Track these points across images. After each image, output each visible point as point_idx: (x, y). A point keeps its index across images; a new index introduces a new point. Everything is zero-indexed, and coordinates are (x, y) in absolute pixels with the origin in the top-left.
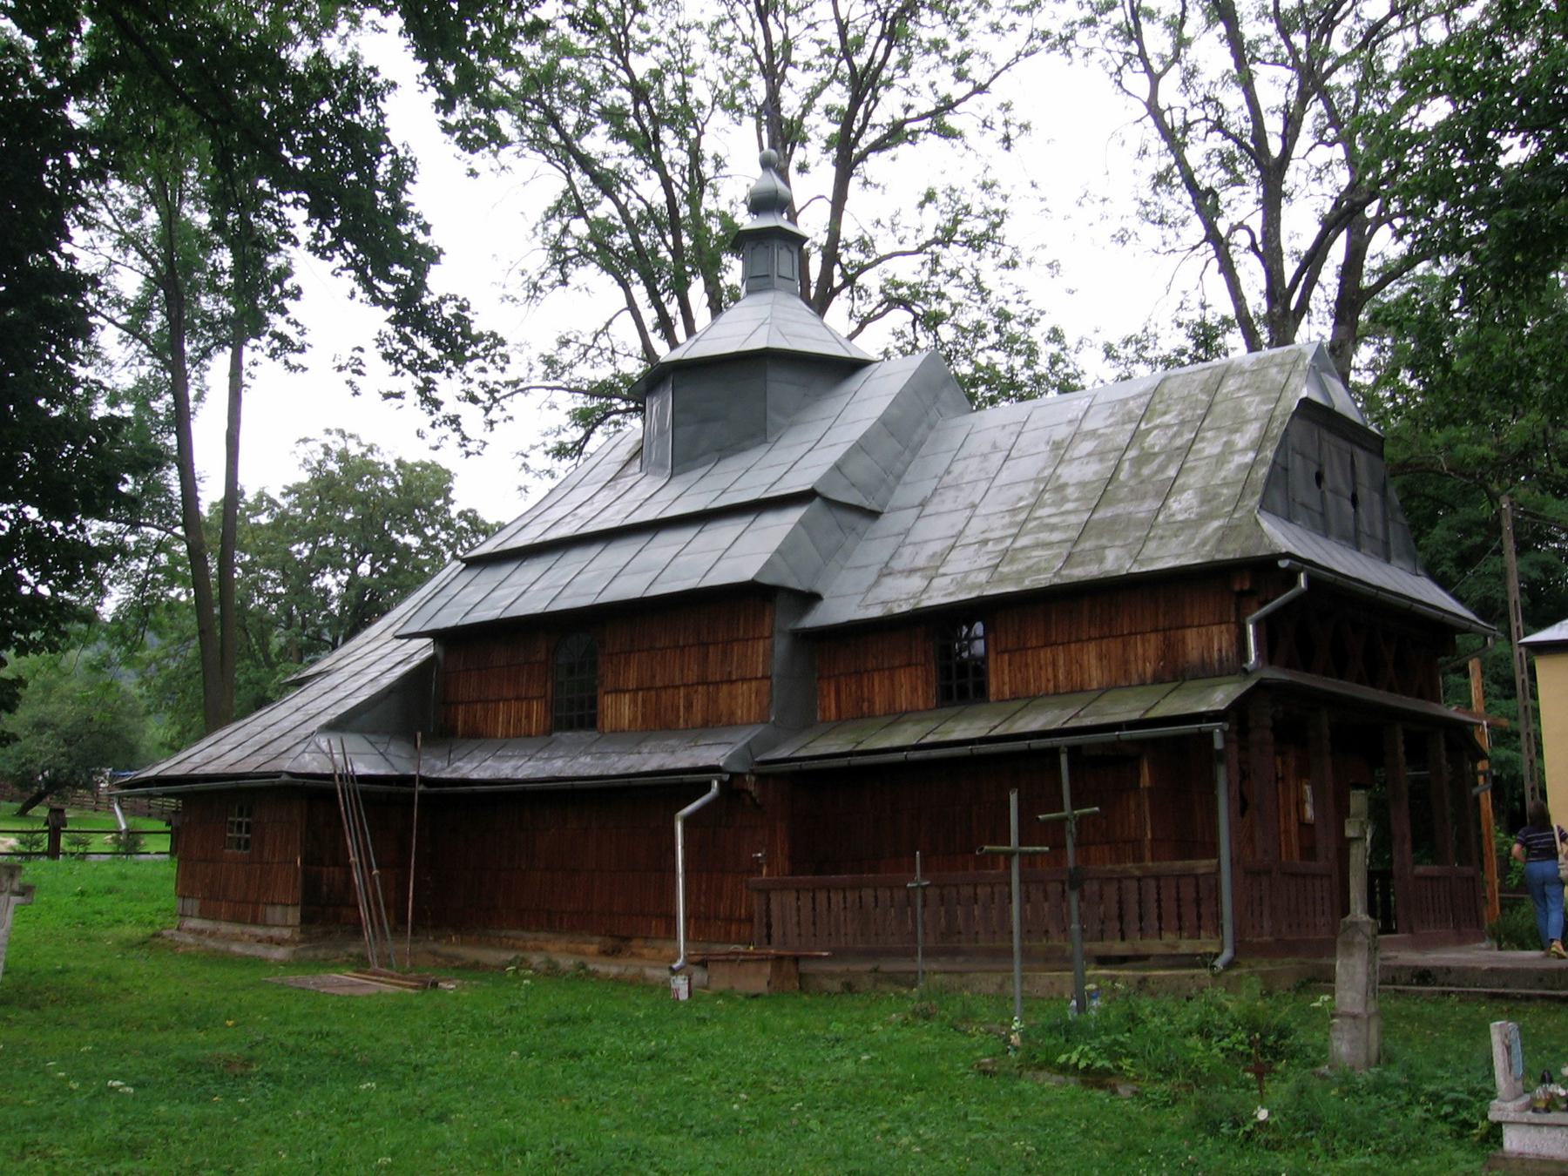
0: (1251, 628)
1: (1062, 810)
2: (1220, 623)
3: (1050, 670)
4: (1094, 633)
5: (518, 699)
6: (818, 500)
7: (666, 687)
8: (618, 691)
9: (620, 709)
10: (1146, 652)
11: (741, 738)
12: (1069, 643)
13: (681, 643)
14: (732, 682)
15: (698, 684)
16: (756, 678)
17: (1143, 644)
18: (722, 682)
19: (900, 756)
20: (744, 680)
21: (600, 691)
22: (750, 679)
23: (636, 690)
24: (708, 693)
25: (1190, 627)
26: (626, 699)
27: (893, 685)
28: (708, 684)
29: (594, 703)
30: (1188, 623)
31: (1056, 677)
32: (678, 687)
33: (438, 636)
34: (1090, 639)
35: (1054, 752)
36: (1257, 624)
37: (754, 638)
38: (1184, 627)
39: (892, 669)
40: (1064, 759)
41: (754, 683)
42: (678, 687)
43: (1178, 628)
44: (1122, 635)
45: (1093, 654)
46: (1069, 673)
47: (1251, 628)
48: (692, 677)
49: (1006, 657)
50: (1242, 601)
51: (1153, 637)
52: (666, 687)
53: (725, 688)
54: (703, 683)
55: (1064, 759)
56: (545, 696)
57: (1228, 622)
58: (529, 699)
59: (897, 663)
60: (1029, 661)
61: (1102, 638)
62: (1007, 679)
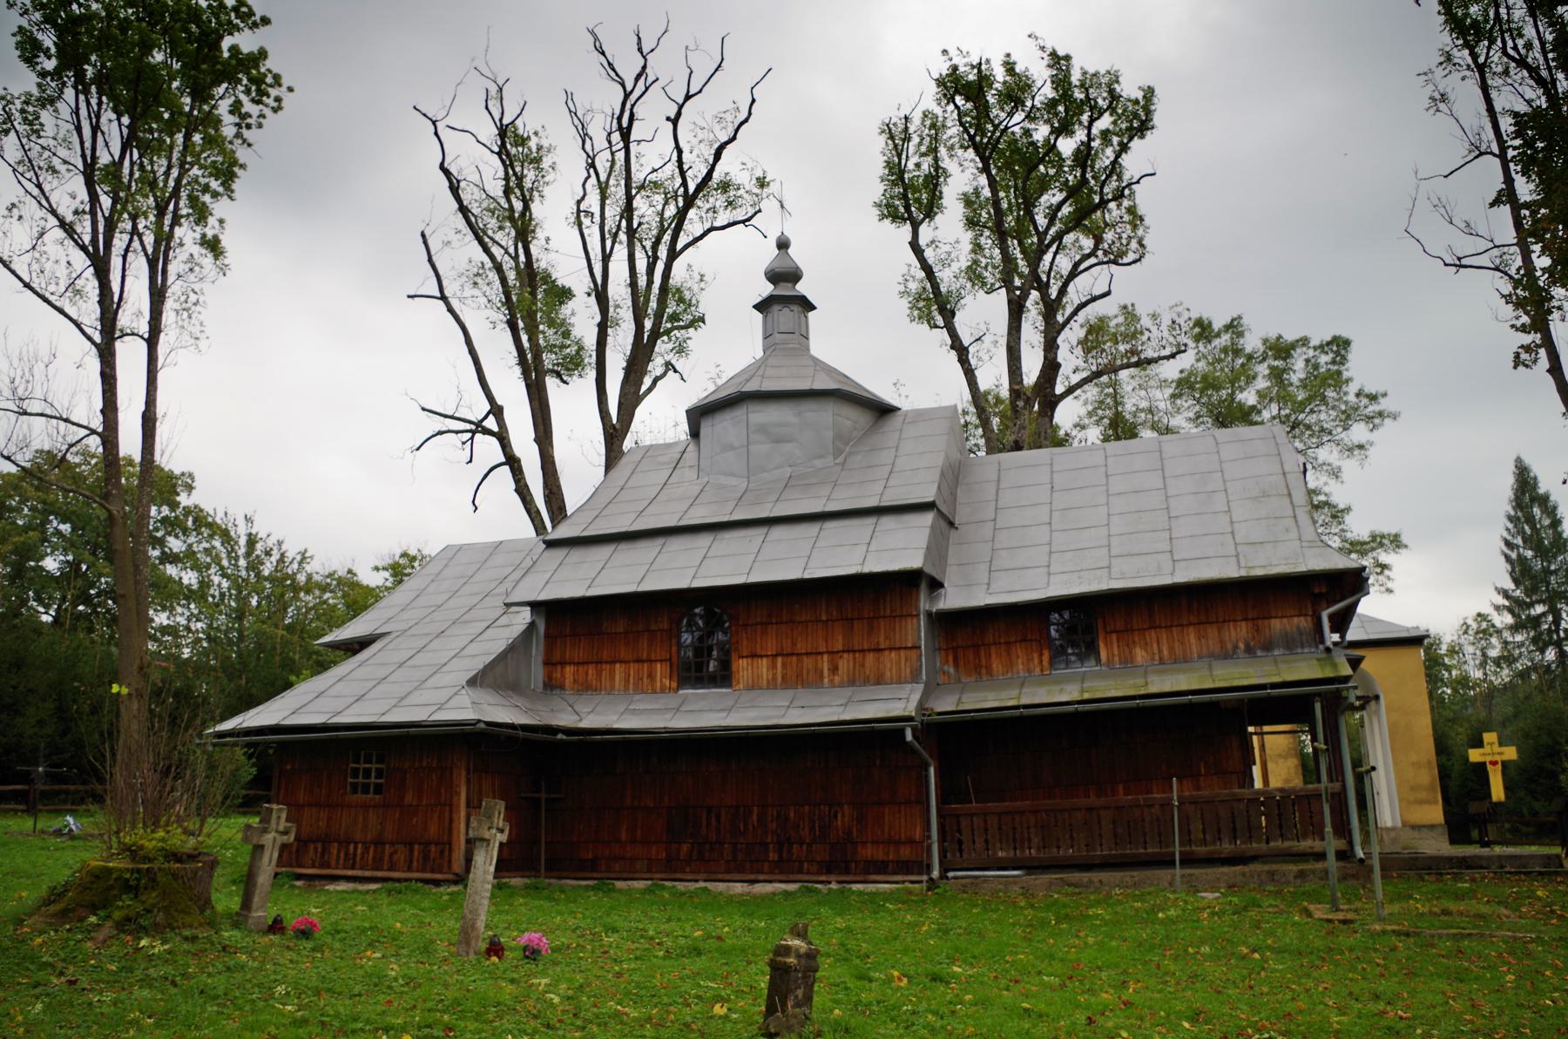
3: (1155, 645)
4: (1193, 619)
5: (638, 661)
7: (807, 654)
8: (753, 656)
10: (1239, 632)
13: (824, 618)
16: (906, 648)
18: (869, 650)
19: (1016, 712)
20: (891, 649)
21: (734, 656)
22: (900, 648)
24: (854, 659)
26: (764, 663)
28: (854, 651)
31: (1160, 651)
32: (821, 653)
33: (535, 606)
34: (1190, 624)
37: (901, 616)
38: (1270, 618)
39: (1008, 643)
40: (1318, 706)
41: (902, 652)
42: (821, 653)
43: (1264, 618)
51: (1243, 623)
52: (807, 654)
53: (870, 657)
54: (848, 651)
55: (1318, 706)
56: (670, 660)
57: (1306, 615)
59: (1013, 639)
62: (1116, 652)
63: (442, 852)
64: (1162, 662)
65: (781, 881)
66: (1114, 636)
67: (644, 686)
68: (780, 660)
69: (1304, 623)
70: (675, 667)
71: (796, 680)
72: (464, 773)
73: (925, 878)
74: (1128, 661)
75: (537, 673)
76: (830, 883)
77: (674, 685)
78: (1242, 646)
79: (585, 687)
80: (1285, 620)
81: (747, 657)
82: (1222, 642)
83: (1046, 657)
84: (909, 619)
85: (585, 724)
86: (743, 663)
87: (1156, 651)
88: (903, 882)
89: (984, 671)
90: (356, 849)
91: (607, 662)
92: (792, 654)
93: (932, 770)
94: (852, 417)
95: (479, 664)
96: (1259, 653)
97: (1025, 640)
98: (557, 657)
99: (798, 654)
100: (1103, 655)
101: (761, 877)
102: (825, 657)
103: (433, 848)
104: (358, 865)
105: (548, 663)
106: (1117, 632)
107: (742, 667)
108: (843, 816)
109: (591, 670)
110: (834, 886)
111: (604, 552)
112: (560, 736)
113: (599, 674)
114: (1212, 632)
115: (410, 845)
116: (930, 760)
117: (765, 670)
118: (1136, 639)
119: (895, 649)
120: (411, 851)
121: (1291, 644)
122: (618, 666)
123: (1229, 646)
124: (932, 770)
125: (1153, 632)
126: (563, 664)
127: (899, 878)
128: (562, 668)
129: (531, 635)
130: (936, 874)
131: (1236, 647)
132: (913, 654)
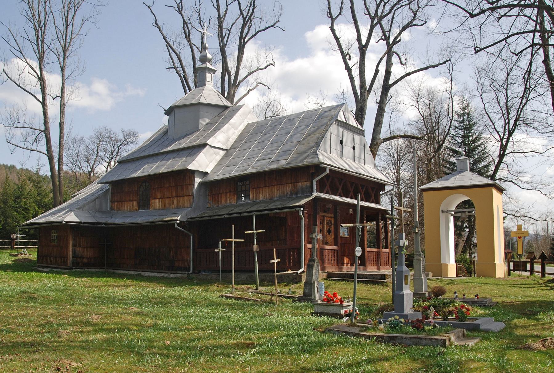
0: (315, 183)
1: (253, 230)
2: (307, 181)
5: (130, 201)
6: (208, 146)
7: (167, 198)
8: (155, 199)
9: (155, 203)
11: (185, 212)
12: (270, 186)
14: (184, 196)
15: (175, 197)
17: (288, 187)
20: (186, 196)
21: (151, 199)
23: (160, 199)
25: (300, 182)
26: (157, 201)
27: (226, 197)
28: (178, 197)
29: (149, 201)
30: (299, 181)
31: (266, 195)
36: (316, 182)
38: (298, 182)
42: (170, 197)
43: (297, 183)
44: (283, 184)
45: (276, 189)
46: (269, 194)
47: (315, 183)
48: (174, 195)
49: (254, 189)
50: (313, 176)
51: (291, 184)
54: (176, 197)
58: (133, 201)
60: (260, 191)
61: (278, 185)
62: (254, 196)
69: (308, 183)
72: (71, 237)
73: (187, 273)
78: (289, 193)
86: (153, 200)
87: (265, 195)
89: (219, 203)
91: (124, 201)
92: (164, 198)
93: (191, 237)
94: (219, 110)
97: (230, 192)
99: (165, 198)
101: (154, 271)
106: (255, 188)
112: (103, 225)
113: (122, 204)
114: (281, 187)
116: (190, 234)
124: (191, 237)
125: (265, 188)
127: (184, 272)
130: (191, 271)
132: (192, 197)
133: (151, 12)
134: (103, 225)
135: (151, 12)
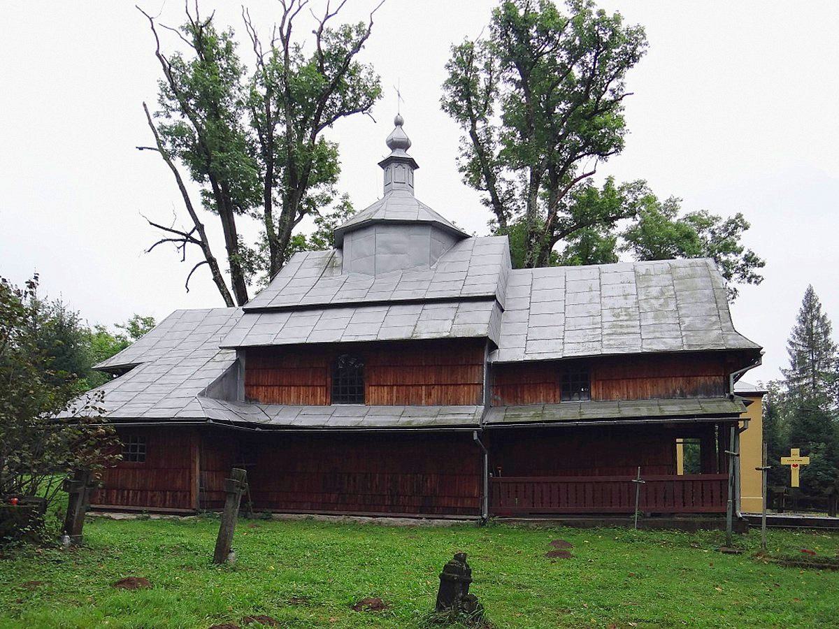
10: (677, 384)
18: (451, 385)
20: (464, 384)
22: (469, 384)
25: (701, 376)
28: (441, 385)
30: (700, 374)
31: (628, 393)
33: (238, 349)
35: (713, 423)
41: (472, 386)
51: (681, 378)
54: (438, 385)
56: (326, 386)
63: (185, 496)
64: (628, 399)
65: (391, 517)
66: (601, 383)
67: (311, 401)
68: (395, 387)
69: (719, 380)
70: (329, 391)
71: (406, 401)
74: (608, 398)
75: (242, 391)
76: (421, 518)
77: (329, 400)
78: (678, 391)
79: (271, 401)
80: (707, 378)
81: (374, 386)
82: (667, 389)
83: (558, 393)
84: (477, 367)
85: (275, 421)
86: (372, 389)
87: (626, 393)
88: (465, 520)
90: (128, 493)
92: (403, 385)
93: (486, 456)
95: (205, 383)
96: (689, 397)
98: (253, 381)
99: (407, 385)
100: (593, 393)
102: (424, 387)
103: (179, 494)
104: (130, 504)
105: (246, 385)
107: (372, 392)
108: (431, 481)
109: (276, 390)
110: (424, 520)
111: (284, 316)
112: (257, 429)
113: (281, 395)
114: (661, 382)
115: (165, 492)
117: (386, 394)
118: (614, 385)
119: (467, 384)
120: (165, 495)
121: (709, 392)
122: (292, 388)
123: (671, 391)
124: (486, 456)
125: (624, 381)
126: (258, 385)
128: (257, 389)
129: (237, 367)
131: (675, 392)
132: (479, 388)
133: (152, 28)
134: (257, 429)
135: (152, 28)
